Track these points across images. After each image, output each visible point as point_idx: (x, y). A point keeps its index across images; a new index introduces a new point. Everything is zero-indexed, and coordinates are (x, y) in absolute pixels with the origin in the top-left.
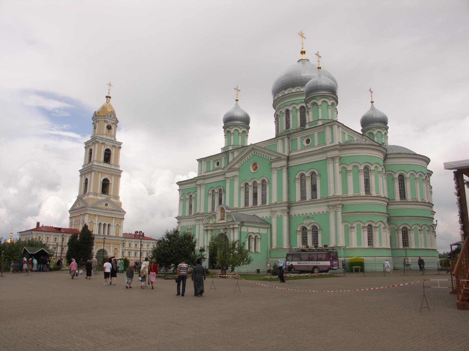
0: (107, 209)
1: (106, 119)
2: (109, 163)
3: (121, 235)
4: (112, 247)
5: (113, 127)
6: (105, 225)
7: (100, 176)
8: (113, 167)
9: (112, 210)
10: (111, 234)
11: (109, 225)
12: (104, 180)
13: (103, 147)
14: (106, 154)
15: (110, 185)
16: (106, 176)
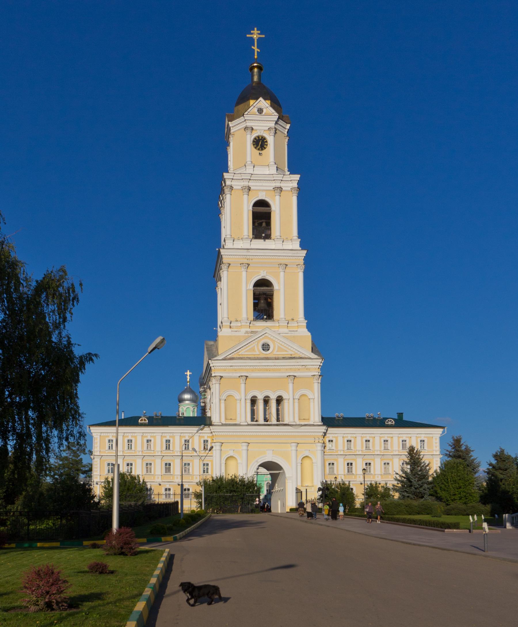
2: (268, 237)
9: (284, 358)
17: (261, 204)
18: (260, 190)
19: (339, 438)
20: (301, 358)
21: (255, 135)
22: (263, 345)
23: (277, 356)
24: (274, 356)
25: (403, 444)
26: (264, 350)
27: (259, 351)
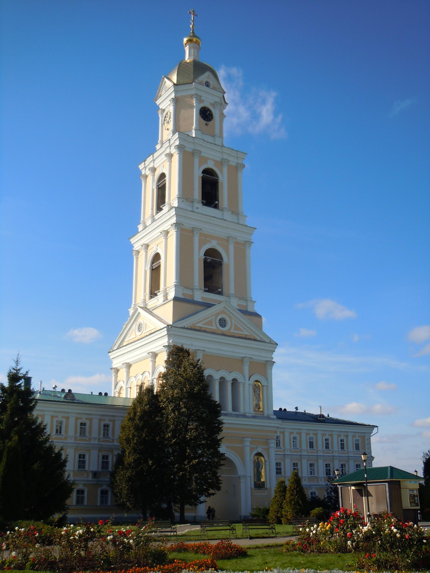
1: (200, 93)
2: (216, 207)
4: (247, 450)
5: (216, 113)
6: (222, 380)
7: (196, 239)
11: (235, 381)
13: (196, 160)
15: (224, 267)
16: (213, 244)
18: (209, 159)
19: (286, 433)
20: (255, 340)
21: (202, 105)
22: (220, 320)
23: (234, 334)
24: (230, 334)
25: (341, 444)
26: (220, 325)
27: (215, 326)
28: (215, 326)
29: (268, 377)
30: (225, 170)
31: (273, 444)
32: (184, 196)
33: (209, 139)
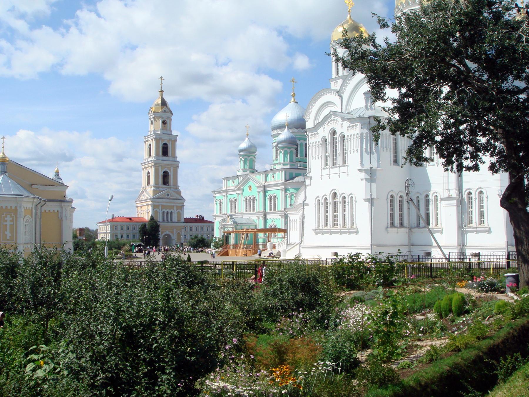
0: (168, 199)
3: (183, 221)
4: (175, 232)
5: (168, 121)
8: (171, 159)
10: (173, 221)
11: (171, 212)
12: (165, 172)
13: (160, 141)
14: (163, 148)
17: (165, 144)
27: (166, 196)
28: (166, 196)
29: (182, 210)
30: (170, 142)
31: (183, 230)
32: (157, 155)
33: (165, 132)
